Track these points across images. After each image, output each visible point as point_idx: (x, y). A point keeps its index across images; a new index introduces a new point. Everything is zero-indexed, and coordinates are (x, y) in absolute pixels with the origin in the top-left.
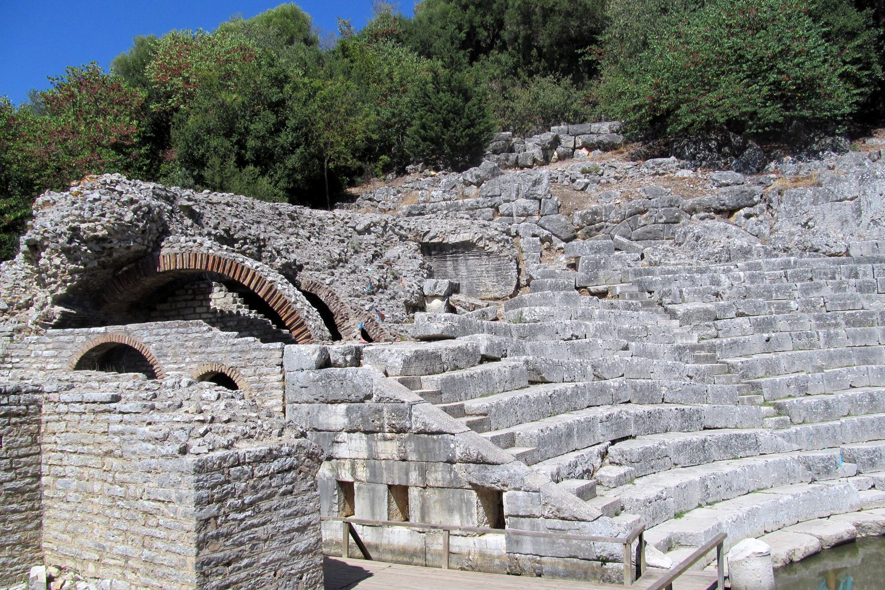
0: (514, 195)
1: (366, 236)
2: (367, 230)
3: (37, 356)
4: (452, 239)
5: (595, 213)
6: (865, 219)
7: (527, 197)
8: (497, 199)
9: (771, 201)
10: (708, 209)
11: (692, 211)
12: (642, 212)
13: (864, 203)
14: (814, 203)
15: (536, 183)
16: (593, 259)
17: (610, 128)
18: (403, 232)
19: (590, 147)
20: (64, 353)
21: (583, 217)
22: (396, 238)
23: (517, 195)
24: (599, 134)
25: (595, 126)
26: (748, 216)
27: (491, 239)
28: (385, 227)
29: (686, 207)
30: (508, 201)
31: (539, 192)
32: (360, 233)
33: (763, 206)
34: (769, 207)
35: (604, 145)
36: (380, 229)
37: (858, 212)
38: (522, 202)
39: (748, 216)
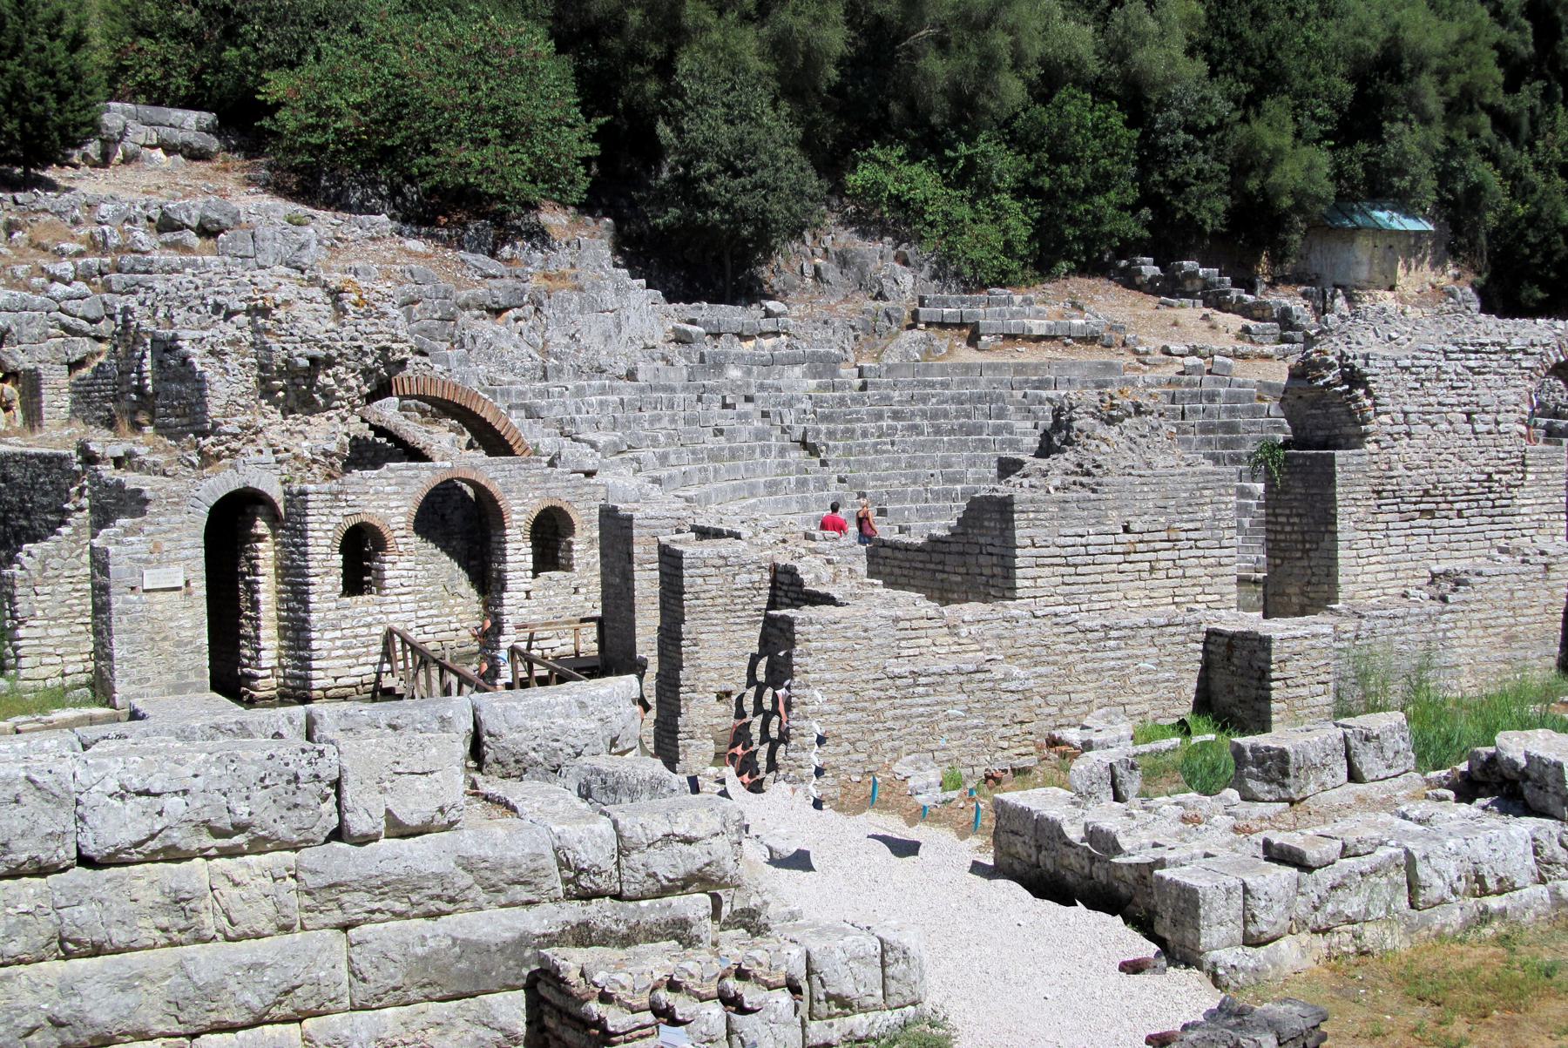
0: (271, 259)
3: (377, 493)
6: (624, 336)
7: (287, 265)
9: (541, 303)
10: (480, 307)
11: (466, 306)
12: (415, 302)
13: (623, 317)
14: (581, 312)
17: (198, 122)
19: (170, 149)
20: (408, 489)
24: (181, 128)
25: (177, 115)
26: (517, 319)
29: (460, 301)
31: (305, 260)
33: (532, 308)
34: (537, 310)
35: (192, 149)
37: (619, 326)
39: (517, 319)
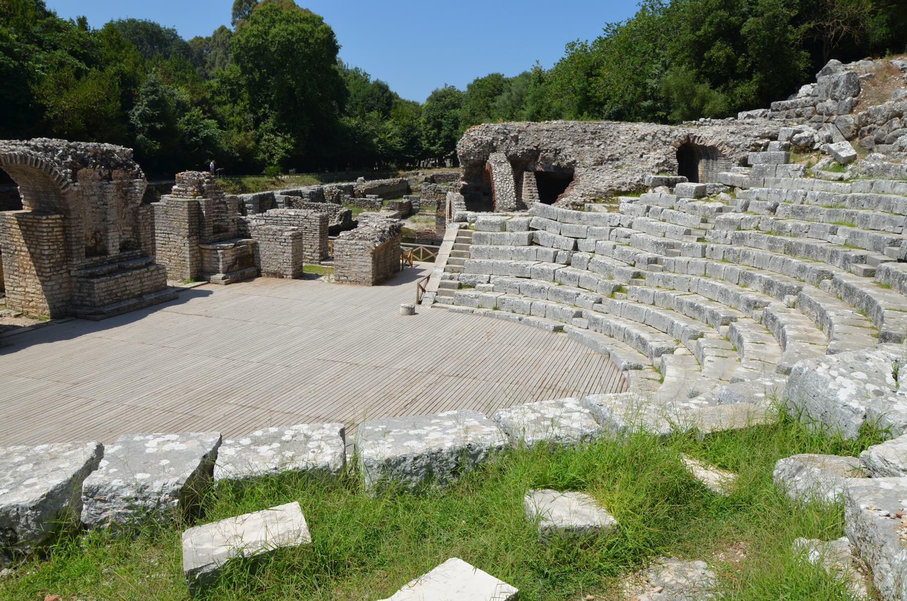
1: (642, 143)
2: (642, 139)
4: (709, 144)
5: (868, 115)
8: (816, 99)
15: (836, 85)
16: (760, 167)
18: (669, 139)
21: (860, 118)
22: (660, 144)
23: (827, 96)
27: (727, 144)
28: (653, 137)
30: (821, 101)
32: (640, 140)
36: (649, 138)
38: (829, 103)
